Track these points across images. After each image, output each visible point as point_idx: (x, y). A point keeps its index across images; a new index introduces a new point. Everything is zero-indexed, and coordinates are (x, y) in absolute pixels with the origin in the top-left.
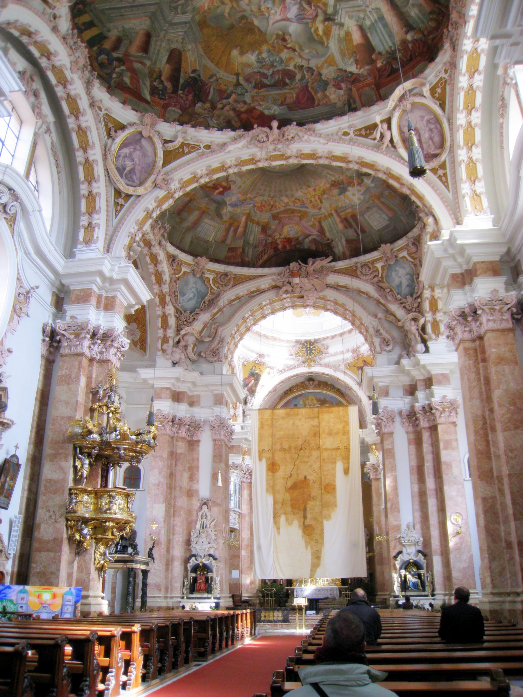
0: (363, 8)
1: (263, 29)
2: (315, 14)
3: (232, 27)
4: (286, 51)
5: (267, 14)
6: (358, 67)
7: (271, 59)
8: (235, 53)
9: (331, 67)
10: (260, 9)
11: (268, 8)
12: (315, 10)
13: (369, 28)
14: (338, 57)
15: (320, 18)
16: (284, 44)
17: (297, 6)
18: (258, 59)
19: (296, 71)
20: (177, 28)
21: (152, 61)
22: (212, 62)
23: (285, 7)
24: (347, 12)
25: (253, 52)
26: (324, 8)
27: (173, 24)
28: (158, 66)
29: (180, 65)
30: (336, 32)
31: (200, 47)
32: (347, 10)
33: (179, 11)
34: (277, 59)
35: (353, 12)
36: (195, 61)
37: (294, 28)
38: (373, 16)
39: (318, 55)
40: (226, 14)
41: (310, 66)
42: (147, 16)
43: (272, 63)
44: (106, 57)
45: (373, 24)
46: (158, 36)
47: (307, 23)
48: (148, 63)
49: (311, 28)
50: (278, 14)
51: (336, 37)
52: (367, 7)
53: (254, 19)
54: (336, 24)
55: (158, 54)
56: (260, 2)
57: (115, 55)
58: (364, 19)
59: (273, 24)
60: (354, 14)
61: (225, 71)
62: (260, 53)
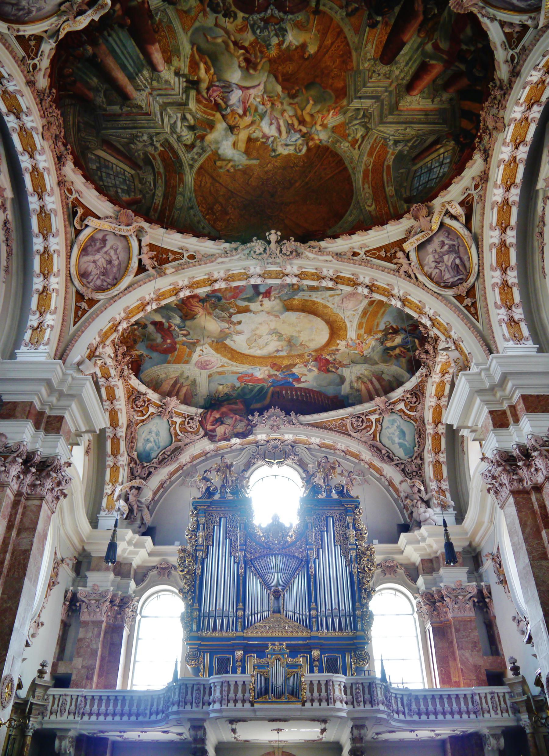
0: (155, 93)
1: (272, 79)
2: (210, 92)
3: (309, 86)
4: (246, 44)
5: (265, 97)
6: (146, 5)
7: (266, 33)
8: (312, 49)
9: (186, 9)
10: (273, 104)
11: (263, 104)
12: (210, 96)
13: (143, 66)
14: (177, 25)
15: (204, 86)
16: (248, 55)
17: (231, 103)
18: (283, 36)
19: (233, 8)
20: (372, 92)
21: (423, 50)
22: (345, 38)
23: (244, 103)
24: (173, 89)
25: (288, 47)
26: (201, 97)
27: (376, 98)
28: (419, 40)
29: (387, 40)
30: (184, 65)
31: (355, 63)
32: (173, 93)
33: (362, 113)
34: (258, 31)
35: (166, 89)
36: (367, 43)
37: (235, 76)
38: (142, 82)
39: (204, 31)
40: (311, 102)
41: (215, 15)
42: (401, 111)
43: (265, 28)
44: (474, 70)
45: (140, 71)
46: (398, 85)
47: (219, 80)
48: (429, 47)
49: (215, 73)
50: (253, 96)
51: (182, 58)
52: (150, 94)
53: (280, 93)
54: (184, 76)
55: (410, 59)
56: (271, 112)
57: (463, 67)
58: (152, 80)
59: (259, 85)
60: (164, 87)
61: (331, 19)
62: (280, 44)
